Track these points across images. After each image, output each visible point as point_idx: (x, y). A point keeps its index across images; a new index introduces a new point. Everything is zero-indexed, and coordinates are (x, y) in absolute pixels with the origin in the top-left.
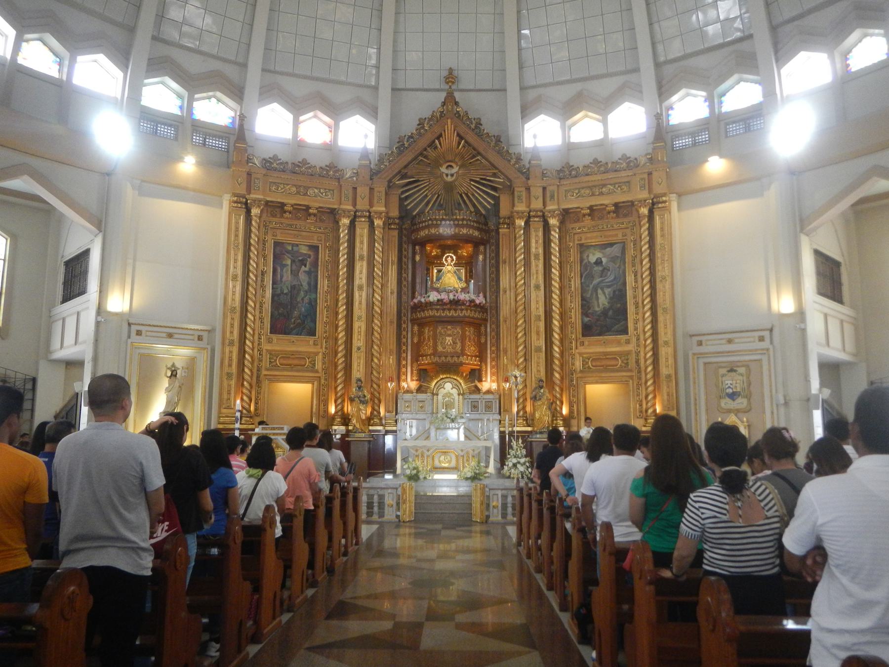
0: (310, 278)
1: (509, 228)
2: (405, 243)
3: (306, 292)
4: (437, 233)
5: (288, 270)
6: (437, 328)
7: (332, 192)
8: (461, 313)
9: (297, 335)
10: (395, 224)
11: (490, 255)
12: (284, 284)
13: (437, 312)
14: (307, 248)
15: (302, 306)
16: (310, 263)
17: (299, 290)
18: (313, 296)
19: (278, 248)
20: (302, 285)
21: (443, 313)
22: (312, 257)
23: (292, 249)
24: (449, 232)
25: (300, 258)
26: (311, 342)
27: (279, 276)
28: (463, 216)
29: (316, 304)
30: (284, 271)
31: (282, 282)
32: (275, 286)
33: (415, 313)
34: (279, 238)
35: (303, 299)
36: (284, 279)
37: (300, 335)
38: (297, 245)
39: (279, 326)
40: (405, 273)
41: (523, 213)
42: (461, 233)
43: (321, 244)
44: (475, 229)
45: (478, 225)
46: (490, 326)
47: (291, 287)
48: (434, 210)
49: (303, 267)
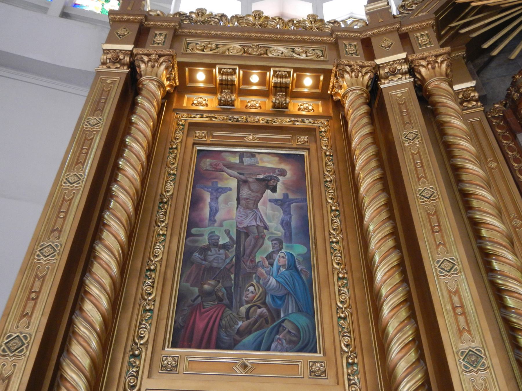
0: (287, 212)
3: (279, 243)
5: (226, 202)
7: (320, 53)
9: (258, 349)
10: (472, 100)
12: (221, 225)
14: (277, 159)
15: (268, 273)
16: (284, 184)
17: (259, 239)
18: (299, 249)
19: (208, 161)
20: (266, 228)
22: (289, 175)
23: (241, 161)
25: (261, 177)
26: (303, 369)
27: (207, 212)
29: (310, 267)
30: (222, 198)
31: (215, 221)
32: (194, 231)
34: (208, 142)
35: (270, 257)
36: (218, 217)
37: (268, 349)
38: (253, 155)
39: (200, 325)
43: (308, 149)
47: (238, 232)
49: (268, 191)
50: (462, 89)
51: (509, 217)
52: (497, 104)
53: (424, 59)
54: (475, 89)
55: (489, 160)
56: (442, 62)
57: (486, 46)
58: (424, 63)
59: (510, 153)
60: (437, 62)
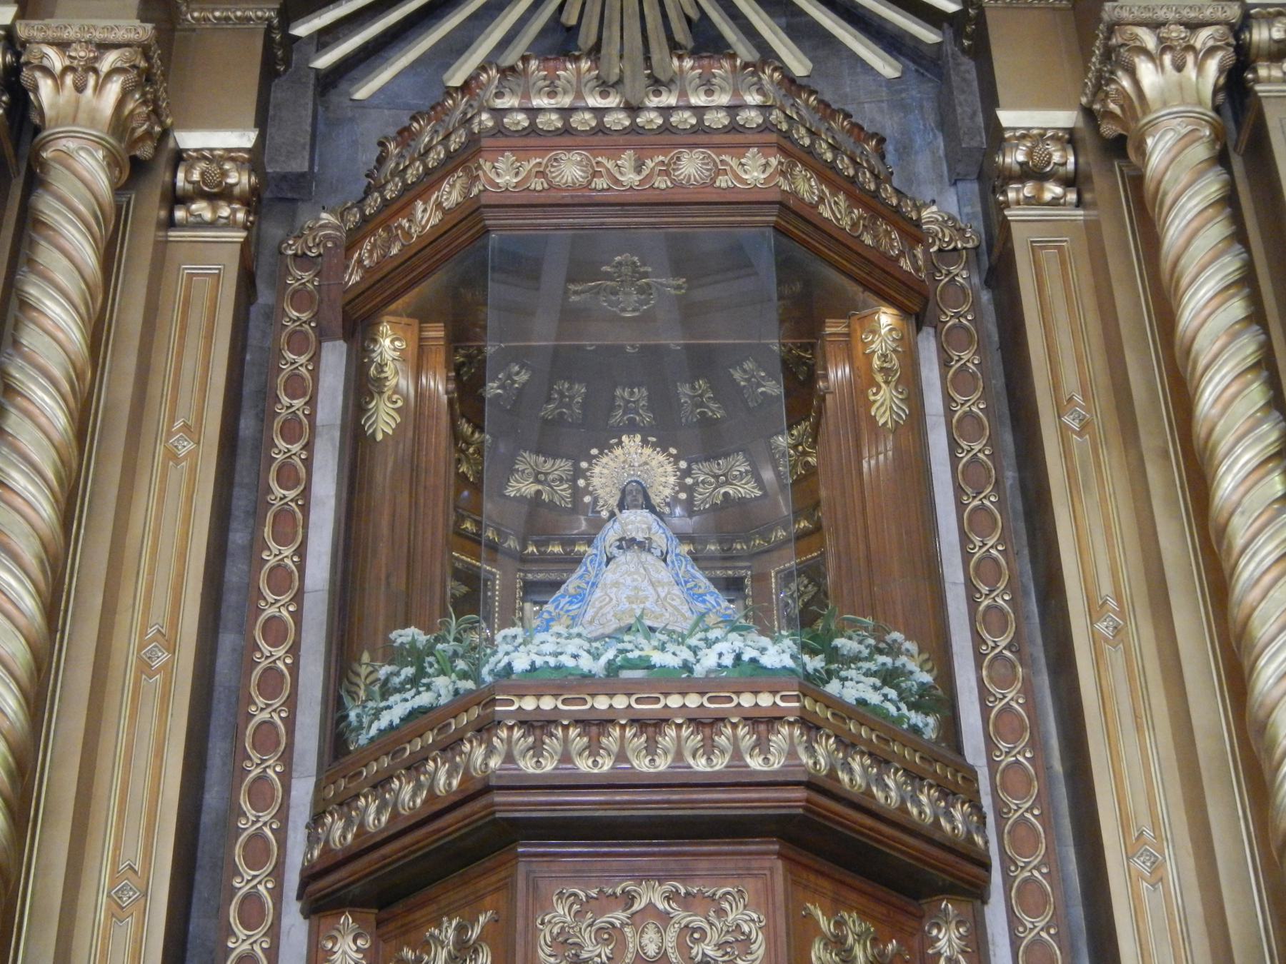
1: (1079, 204)
2: (298, 342)
4: (537, 184)
6: (540, 903)
8: (762, 746)
10: (224, 194)
11: (949, 413)
13: (537, 749)
21: (593, 749)
24: (630, 178)
28: (736, 93)
33: (346, 802)
40: (282, 540)
41: (1193, 26)
42: (722, 182)
44: (835, 189)
45: (843, 164)
46: (1013, 921)
48: (511, 57)
50: (211, 150)
51: (143, 633)
52: (332, 212)
53: (62, 46)
54: (254, 159)
55: (178, 424)
56: (115, 71)
57: (302, 30)
58: (56, 60)
59: (285, 400)
60: (96, 71)
